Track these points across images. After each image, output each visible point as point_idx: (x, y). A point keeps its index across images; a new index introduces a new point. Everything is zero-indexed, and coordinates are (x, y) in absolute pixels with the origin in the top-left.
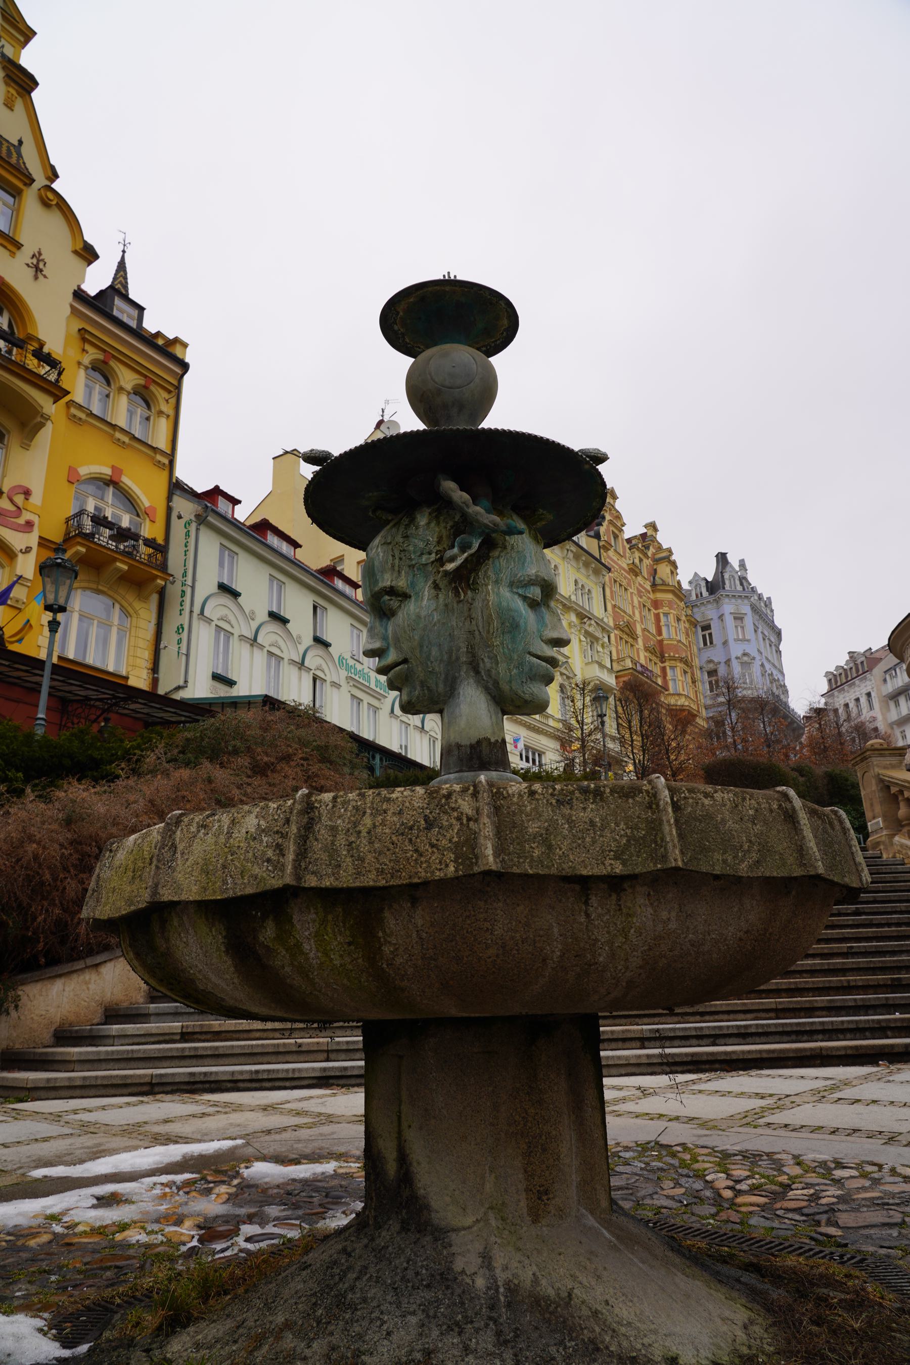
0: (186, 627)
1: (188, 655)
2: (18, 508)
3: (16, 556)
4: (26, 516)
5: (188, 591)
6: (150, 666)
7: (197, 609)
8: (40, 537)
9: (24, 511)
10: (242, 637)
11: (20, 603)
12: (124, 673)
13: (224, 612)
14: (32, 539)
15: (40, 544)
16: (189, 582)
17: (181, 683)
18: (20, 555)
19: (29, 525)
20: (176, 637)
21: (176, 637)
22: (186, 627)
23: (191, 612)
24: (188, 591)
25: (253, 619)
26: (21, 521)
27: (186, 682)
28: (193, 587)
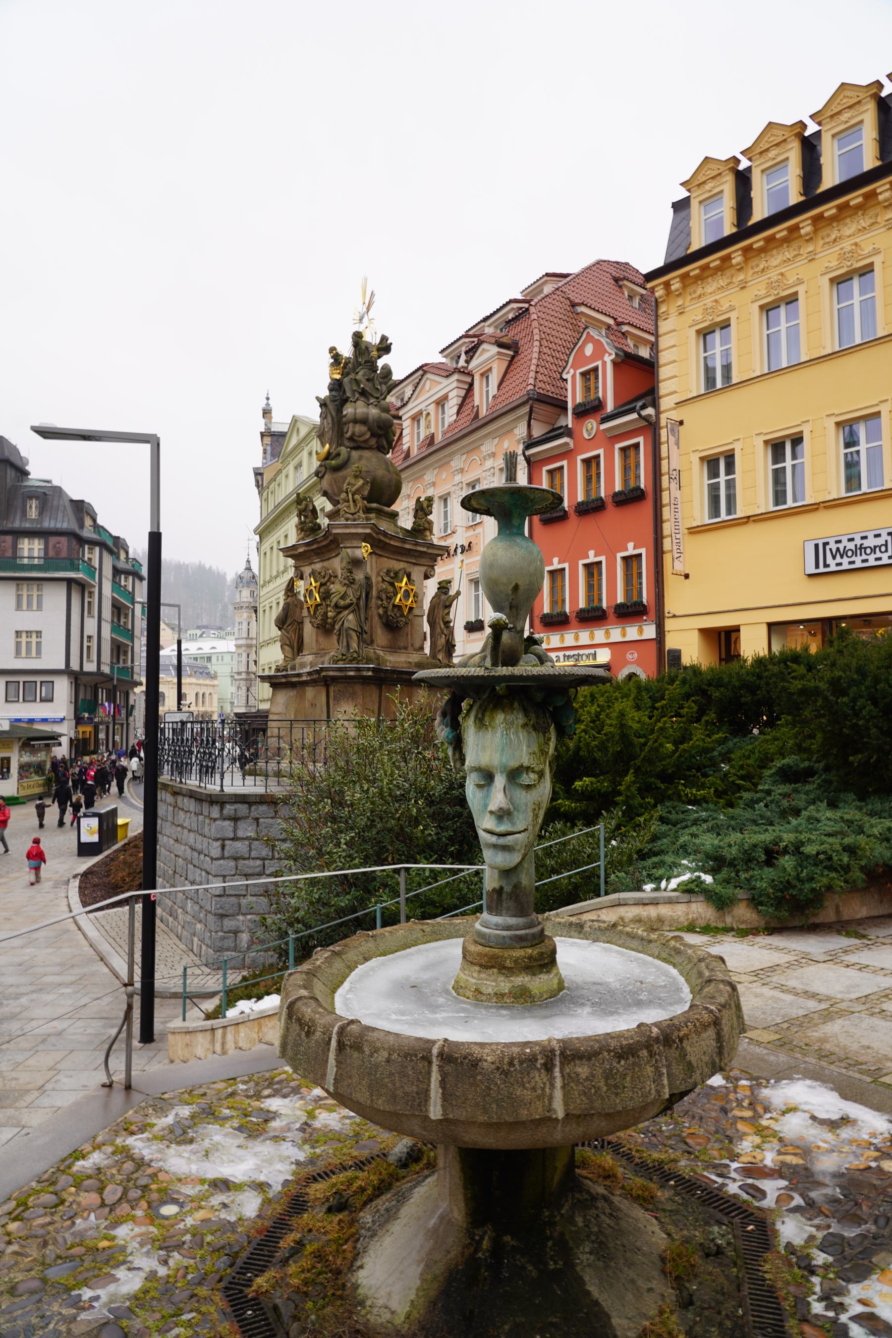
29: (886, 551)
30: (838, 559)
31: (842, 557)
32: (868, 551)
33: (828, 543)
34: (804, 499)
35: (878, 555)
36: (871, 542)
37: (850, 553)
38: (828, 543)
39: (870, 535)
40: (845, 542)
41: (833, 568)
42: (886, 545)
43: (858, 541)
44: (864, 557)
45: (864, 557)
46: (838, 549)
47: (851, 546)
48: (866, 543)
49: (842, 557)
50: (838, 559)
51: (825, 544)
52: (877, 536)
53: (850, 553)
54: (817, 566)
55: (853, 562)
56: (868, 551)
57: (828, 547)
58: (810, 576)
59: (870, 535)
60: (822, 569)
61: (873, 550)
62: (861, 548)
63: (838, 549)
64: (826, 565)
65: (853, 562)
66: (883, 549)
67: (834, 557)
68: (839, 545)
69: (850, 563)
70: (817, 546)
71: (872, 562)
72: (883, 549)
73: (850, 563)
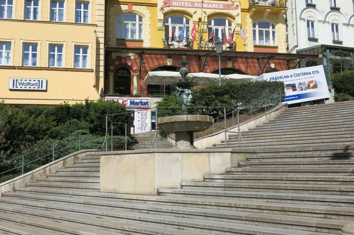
0: (295, 24)
1: (297, 34)
2: (233, 2)
3: (235, 18)
4: (236, 4)
5: (294, 11)
6: (286, 40)
7: (298, 17)
8: (241, 9)
9: (235, 2)
10: (319, 21)
11: (239, 32)
12: (276, 45)
13: (309, 14)
14: (239, 10)
15: (241, 11)
16: (294, 7)
17: (296, 45)
18: (236, 17)
19: (237, 6)
20: (292, 29)
21: (292, 29)
22: (295, 24)
23: (296, 18)
24: (294, 11)
25: (323, 13)
26: (235, 6)
27: (297, 44)
28: (295, 9)
29: (37, 86)
30: (21, 86)
31: (22, 85)
32: (31, 85)
33: (18, 80)
34: (62, 66)
35: (34, 86)
36: (32, 82)
37: (25, 84)
38: (18, 80)
39: (32, 80)
40: (24, 81)
41: (19, 88)
42: (37, 84)
43: (28, 81)
44: (30, 86)
45: (30, 86)
46: (21, 83)
47: (26, 82)
48: (31, 82)
49: (22, 85)
50: (21, 86)
51: (17, 80)
52: (34, 81)
53: (25, 84)
54: (13, 87)
55: (26, 88)
56: (31, 85)
57: (18, 81)
58: (11, 90)
59: (32, 80)
60: (15, 88)
61: (33, 85)
62: (29, 84)
63: (21, 83)
64: (17, 87)
65: (26, 88)
66: (36, 85)
67: (20, 85)
68: (21, 81)
69: (25, 88)
70: (14, 80)
71: (32, 88)
72: (36, 85)
73: (25, 88)
